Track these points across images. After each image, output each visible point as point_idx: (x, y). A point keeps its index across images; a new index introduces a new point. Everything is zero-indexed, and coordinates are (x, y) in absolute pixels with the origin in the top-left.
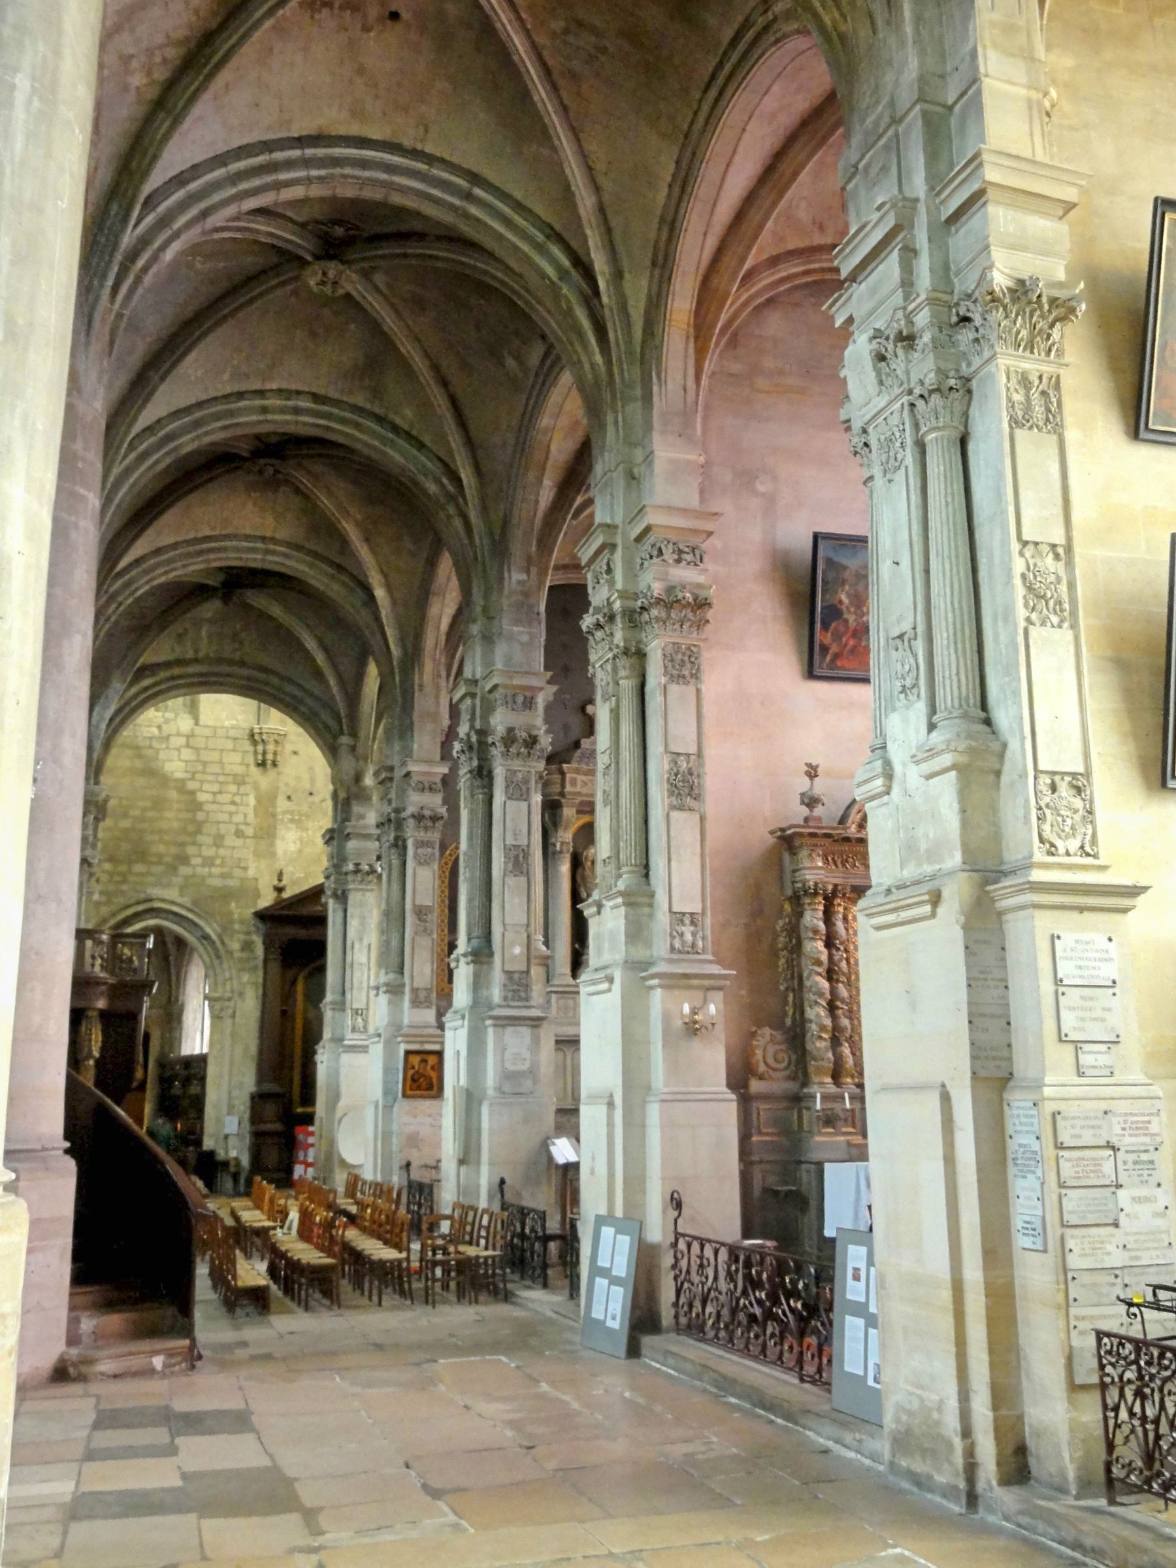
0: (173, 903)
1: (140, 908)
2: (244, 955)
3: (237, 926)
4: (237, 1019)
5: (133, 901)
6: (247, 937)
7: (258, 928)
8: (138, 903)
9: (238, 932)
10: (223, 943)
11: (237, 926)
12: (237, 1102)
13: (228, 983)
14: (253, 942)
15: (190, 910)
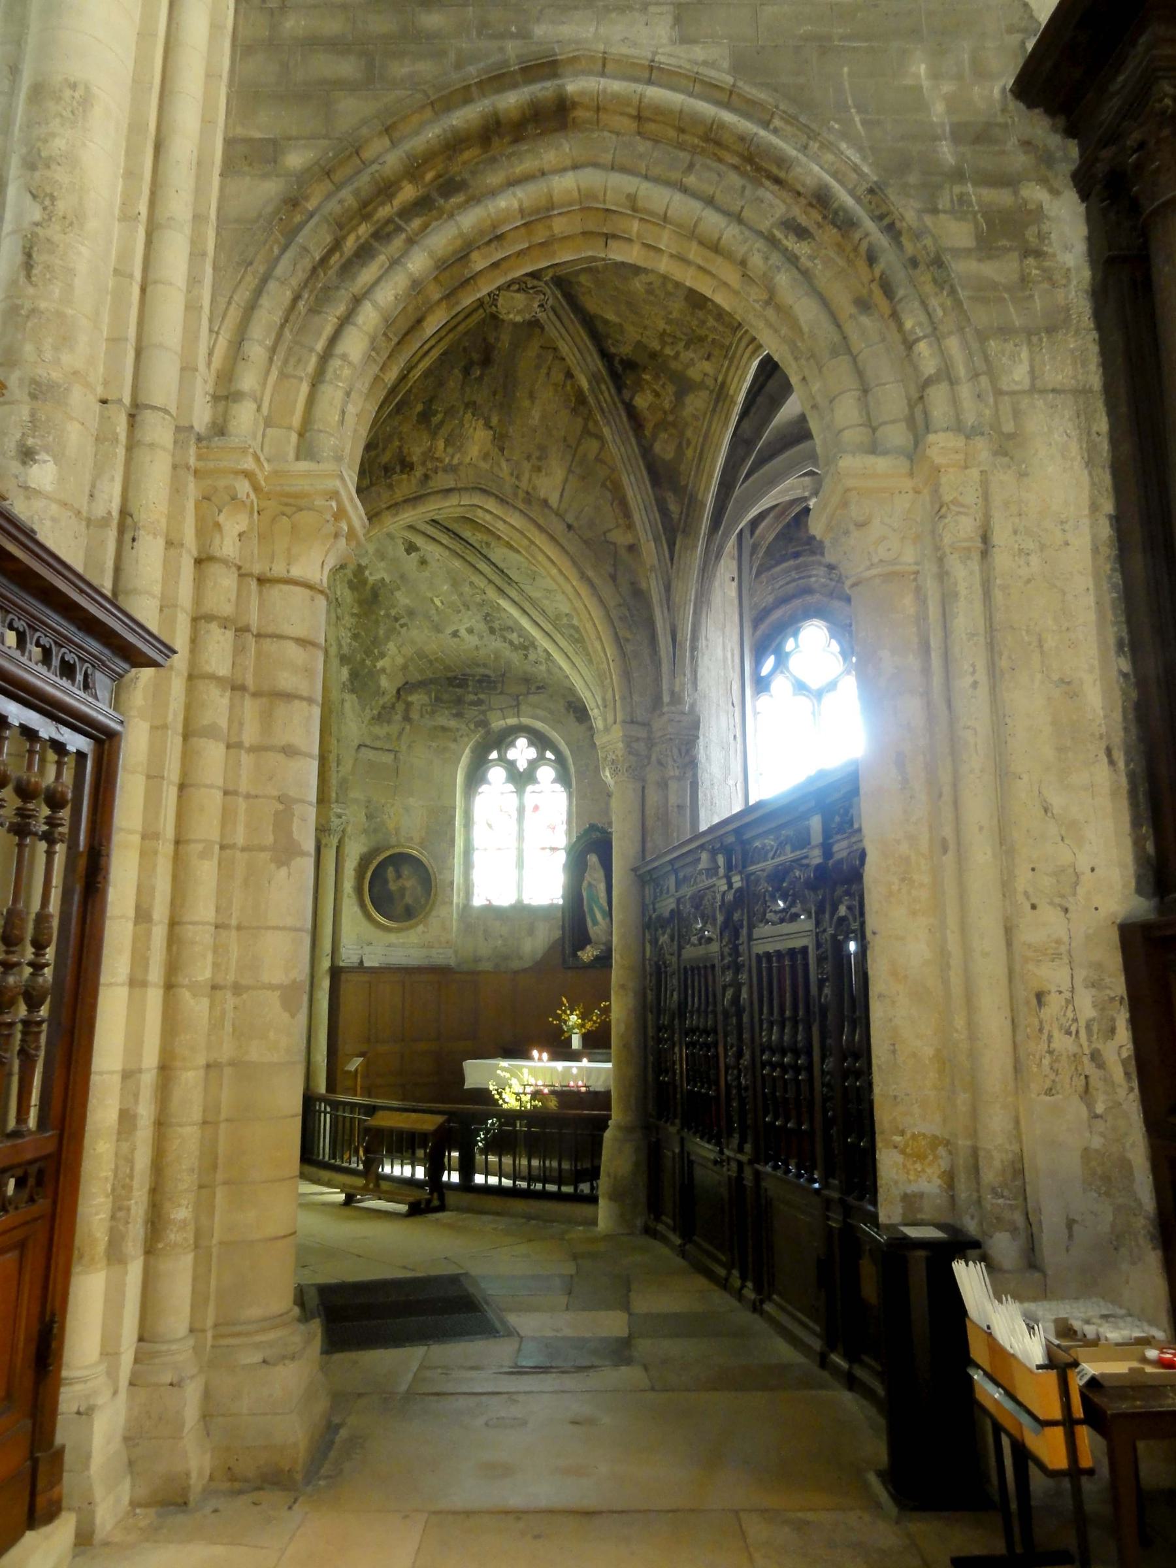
0: (653, 73)
1: (511, 101)
2: (989, 270)
3: (947, 153)
4: (1002, 560)
5: (473, 71)
6: (1002, 197)
7: (1047, 159)
8: (498, 80)
9: (958, 175)
10: (892, 230)
11: (947, 153)
12: (1055, 976)
13: (938, 396)
14: (1037, 214)
15: (728, 98)
